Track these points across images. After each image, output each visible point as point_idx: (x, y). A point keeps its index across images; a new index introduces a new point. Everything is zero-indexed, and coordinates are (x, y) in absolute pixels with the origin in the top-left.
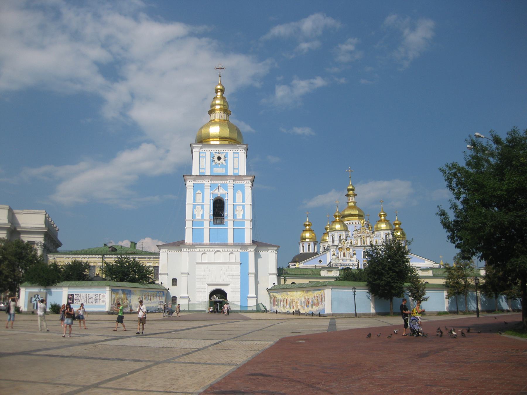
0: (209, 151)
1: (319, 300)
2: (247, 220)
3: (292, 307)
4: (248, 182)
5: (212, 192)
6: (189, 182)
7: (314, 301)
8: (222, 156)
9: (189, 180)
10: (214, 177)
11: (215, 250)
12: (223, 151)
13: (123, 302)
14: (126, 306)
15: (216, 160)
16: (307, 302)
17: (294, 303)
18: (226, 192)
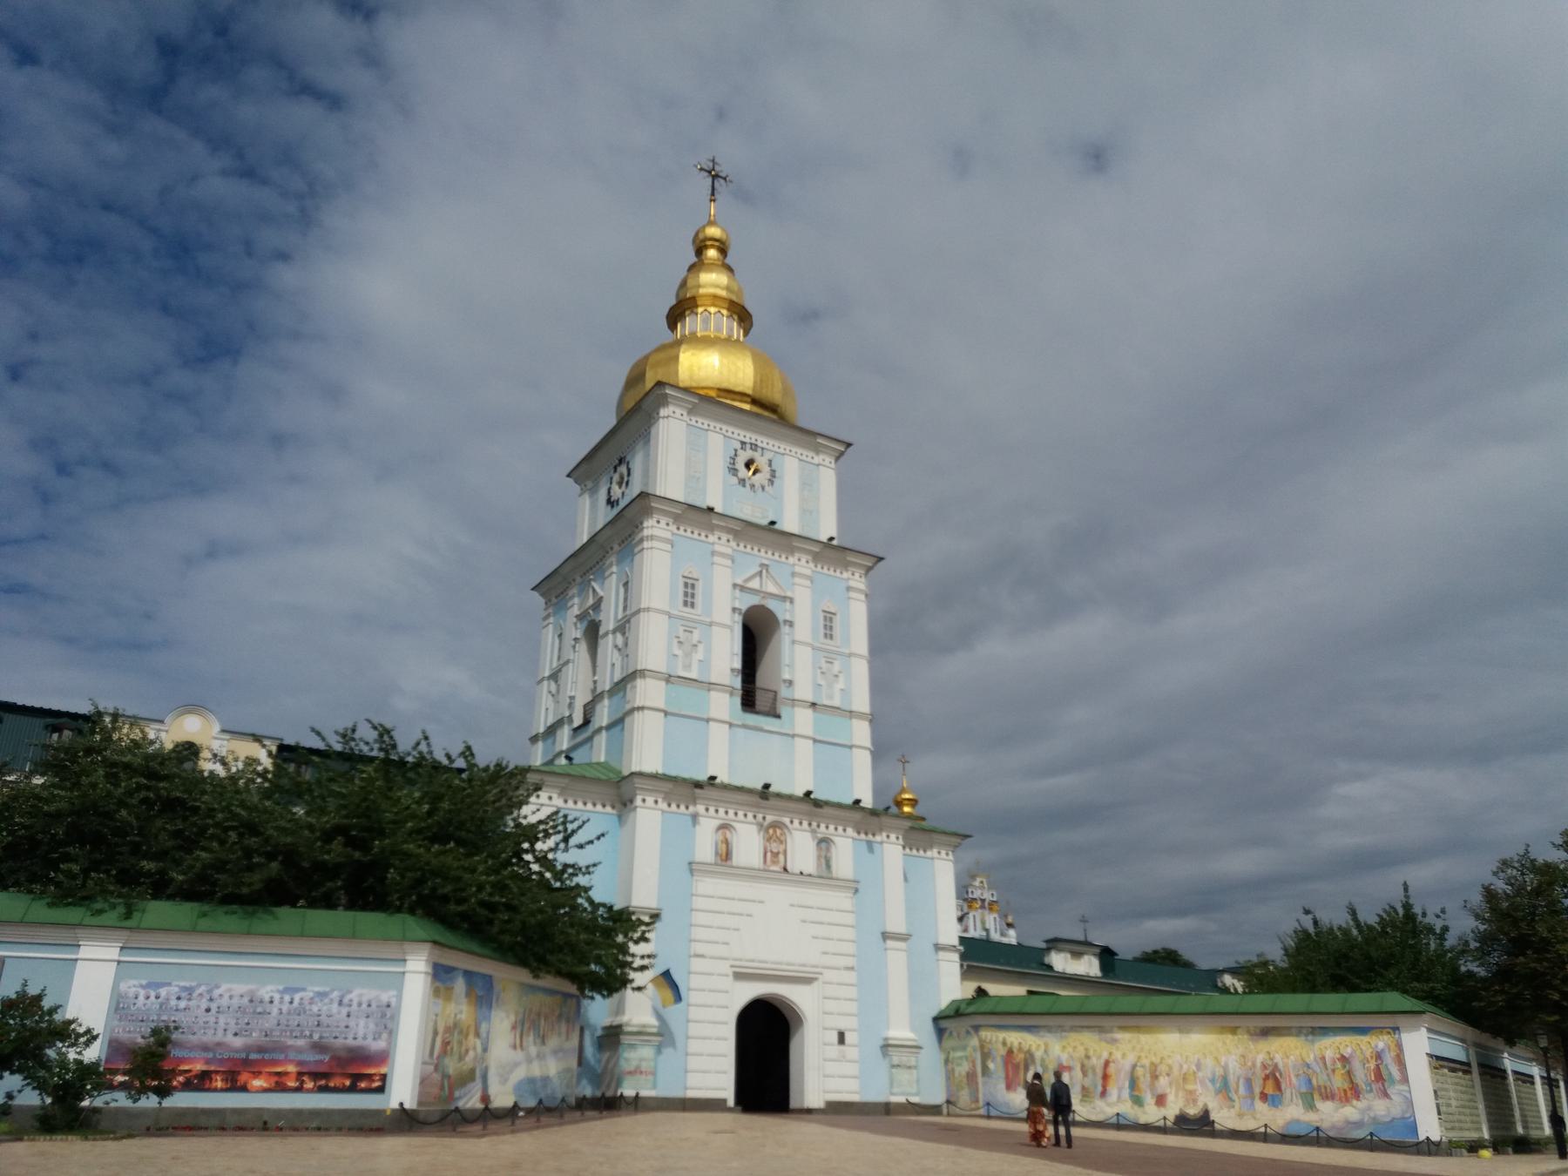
0: (718, 429)
1: (1361, 1076)
2: (860, 716)
3: (1149, 1100)
4: (857, 575)
5: (739, 581)
6: (658, 522)
7: (1320, 1079)
8: (761, 461)
9: (656, 517)
10: (746, 531)
11: (764, 818)
12: (764, 445)
13: (463, 1049)
14: (467, 1078)
15: (743, 473)
16: (1270, 1083)
17: (1163, 1081)
18: (789, 594)
